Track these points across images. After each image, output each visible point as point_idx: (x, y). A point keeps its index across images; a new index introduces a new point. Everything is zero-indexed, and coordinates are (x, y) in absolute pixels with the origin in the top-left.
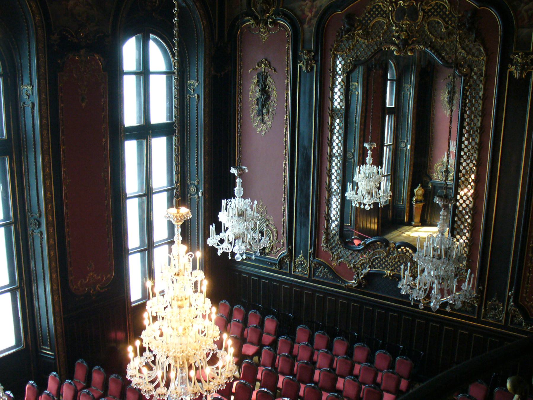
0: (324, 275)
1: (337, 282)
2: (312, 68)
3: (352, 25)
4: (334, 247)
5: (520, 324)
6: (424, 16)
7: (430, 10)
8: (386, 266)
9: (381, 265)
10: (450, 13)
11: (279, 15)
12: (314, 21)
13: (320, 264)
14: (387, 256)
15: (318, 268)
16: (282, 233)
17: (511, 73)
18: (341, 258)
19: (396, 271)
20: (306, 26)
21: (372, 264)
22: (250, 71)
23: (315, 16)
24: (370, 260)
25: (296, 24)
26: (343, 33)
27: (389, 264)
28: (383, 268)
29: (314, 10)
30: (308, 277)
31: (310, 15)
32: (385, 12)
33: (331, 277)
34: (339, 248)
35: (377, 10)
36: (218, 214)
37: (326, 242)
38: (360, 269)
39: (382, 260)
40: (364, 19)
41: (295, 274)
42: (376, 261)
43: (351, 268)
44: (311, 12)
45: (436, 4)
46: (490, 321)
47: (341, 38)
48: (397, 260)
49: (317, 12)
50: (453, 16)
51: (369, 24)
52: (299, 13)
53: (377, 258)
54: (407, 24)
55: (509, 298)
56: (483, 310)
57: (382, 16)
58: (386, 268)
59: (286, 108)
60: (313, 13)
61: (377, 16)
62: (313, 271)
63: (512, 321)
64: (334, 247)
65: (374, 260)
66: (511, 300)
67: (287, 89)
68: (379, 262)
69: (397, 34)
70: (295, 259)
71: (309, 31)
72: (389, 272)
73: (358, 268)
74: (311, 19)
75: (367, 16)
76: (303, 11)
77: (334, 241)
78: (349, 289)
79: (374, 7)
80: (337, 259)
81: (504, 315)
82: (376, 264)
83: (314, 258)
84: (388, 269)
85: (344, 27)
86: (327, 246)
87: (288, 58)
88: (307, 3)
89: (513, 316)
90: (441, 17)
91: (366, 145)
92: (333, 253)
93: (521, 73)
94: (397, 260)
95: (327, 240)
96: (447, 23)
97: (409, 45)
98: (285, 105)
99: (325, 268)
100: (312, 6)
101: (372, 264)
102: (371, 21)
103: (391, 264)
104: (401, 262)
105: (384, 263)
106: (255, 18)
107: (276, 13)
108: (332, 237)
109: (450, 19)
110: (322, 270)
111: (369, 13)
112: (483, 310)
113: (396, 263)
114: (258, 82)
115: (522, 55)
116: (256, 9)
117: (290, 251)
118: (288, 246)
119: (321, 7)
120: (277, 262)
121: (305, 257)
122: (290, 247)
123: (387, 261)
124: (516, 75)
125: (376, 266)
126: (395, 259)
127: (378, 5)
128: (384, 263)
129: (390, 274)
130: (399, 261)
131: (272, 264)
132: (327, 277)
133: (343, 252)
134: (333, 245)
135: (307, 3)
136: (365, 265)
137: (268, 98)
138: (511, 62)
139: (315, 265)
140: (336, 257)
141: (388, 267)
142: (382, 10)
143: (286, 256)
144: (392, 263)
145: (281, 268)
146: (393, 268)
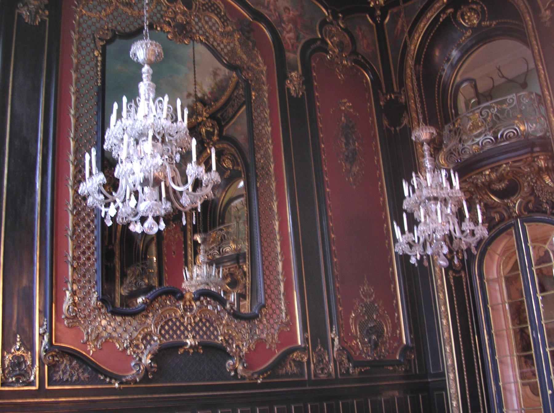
0: (72, 376)
1: (103, 382)
5: (347, 370)
6: (199, 8)
9: (175, 332)
10: (225, 15)
27: (186, 328)
33: (86, 375)
39: (174, 324)
43: (125, 349)
53: (166, 323)
56: (312, 366)
58: (182, 336)
65: (163, 327)
68: (171, 328)
81: (332, 364)
84: (187, 337)
96: (223, 23)
110: (66, 366)
113: (197, 324)
123: (182, 324)
124: (293, 93)
126: (195, 317)
128: (178, 328)
132: (79, 377)
144: (191, 324)
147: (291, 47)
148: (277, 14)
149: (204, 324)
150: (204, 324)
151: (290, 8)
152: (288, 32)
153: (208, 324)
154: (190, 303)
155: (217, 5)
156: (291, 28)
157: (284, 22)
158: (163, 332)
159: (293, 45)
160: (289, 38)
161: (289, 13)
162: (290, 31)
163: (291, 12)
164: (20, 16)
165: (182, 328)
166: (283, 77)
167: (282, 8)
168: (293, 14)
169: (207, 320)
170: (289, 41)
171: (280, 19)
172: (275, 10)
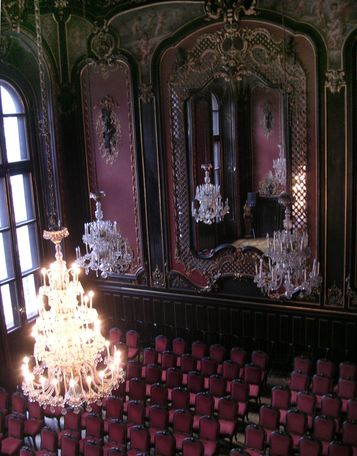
0: (180, 285)
2: (152, 100)
3: (185, 58)
4: (187, 258)
6: (248, 45)
7: (253, 40)
8: (235, 270)
9: (231, 269)
10: (271, 41)
11: (117, 54)
12: (150, 58)
13: (176, 275)
14: (235, 261)
15: (173, 279)
16: (138, 251)
17: (328, 89)
18: (193, 267)
19: (244, 272)
20: (143, 62)
21: (222, 269)
22: (94, 108)
23: (150, 53)
24: (220, 266)
25: (133, 61)
26: (178, 65)
27: (237, 267)
28: (233, 272)
29: (149, 47)
30: (165, 288)
31: (145, 52)
32: (213, 44)
33: (186, 285)
34: (191, 258)
35: (206, 43)
36: (82, 237)
37: (179, 255)
38: (212, 274)
39: (231, 265)
40: (195, 51)
41: (153, 286)
42: (226, 266)
43: (204, 275)
44: (146, 49)
45: (258, 34)
46: (332, 306)
47: (176, 70)
48: (244, 263)
49: (152, 49)
50: (273, 43)
51: (200, 56)
52: (135, 51)
53: (226, 264)
54: (233, 53)
55: (346, 283)
56: (325, 297)
57: (211, 48)
58: (235, 272)
59: (131, 138)
60: (149, 51)
61: (206, 48)
62: (169, 282)
63: (351, 303)
64: (187, 258)
65: (224, 266)
66: (348, 285)
67: (130, 121)
68: (228, 267)
69: (226, 63)
70: (152, 273)
71: (145, 66)
72: (238, 274)
73: (210, 275)
74: (147, 56)
75: (197, 49)
76: (139, 49)
77: (186, 253)
78: (205, 294)
79: (204, 40)
80: (190, 269)
82: (226, 269)
83: (169, 270)
84: (237, 272)
85: (178, 60)
86: (180, 258)
87: (129, 93)
88: (142, 42)
89: (351, 299)
90: (263, 44)
91: (203, 167)
92: (186, 264)
93: (336, 88)
94: (244, 263)
95: (180, 253)
96: (269, 49)
97: (237, 72)
98: (130, 135)
99: (180, 278)
100: (147, 43)
101: (222, 269)
102: (202, 53)
103: (239, 267)
104: (248, 264)
105: (233, 267)
106: (97, 59)
107: (115, 52)
108: (184, 250)
109: (271, 46)
110: (177, 280)
111: (200, 46)
112: (325, 297)
113: (244, 266)
114: (103, 117)
115: (335, 73)
116: (96, 51)
117: (146, 267)
118: (145, 262)
119: (155, 45)
120: (136, 278)
121: (161, 270)
122: (146, 263)
123: (235, 265)
124: (332, 90)
125: (226, 271)
126: (242, 262)
127: (207, 39)
128: (233, 267)
129: (239, 276)
130: (246, 264)
131: (131, 281)
133: (195, 262)
134: (185, 257)
135: (142, 42)
136: (216, 271)
137: (114, 131)
138: (327, 79)
139: (171, 277)
140: (189, 267)
141: (237, 270)
142: (210, 42)
143: (143, 272)
144: (240, 266)
145: (140, 283)
146: (242, 270)
147: (335, 44)
148: (323, 16)
149: (248, 266)
150: (248, 266)
151: (338, 2)
152: (333, 30)
153: (251, 266)
154: (240, 253)
155: (264, 35)
156: (337, 25)
157: (330, 21)
158: (224, 268)
159: (338, 42)
160: (334, 36)
161: (337, 9)
162: (336, 27)
163: (339, 7)
164: (141, 100)
165: (235, 267)
166: (322, 79)
167: (329, 7)
168: (341, 8)
169: (250, 264)
170: (333, 39)
171: (327, 20)
172: (321, 13)
